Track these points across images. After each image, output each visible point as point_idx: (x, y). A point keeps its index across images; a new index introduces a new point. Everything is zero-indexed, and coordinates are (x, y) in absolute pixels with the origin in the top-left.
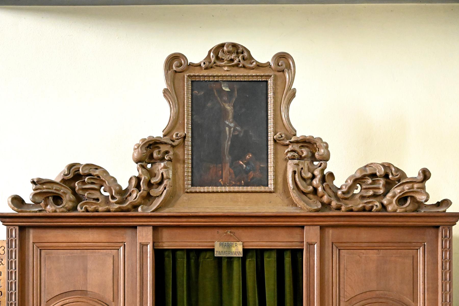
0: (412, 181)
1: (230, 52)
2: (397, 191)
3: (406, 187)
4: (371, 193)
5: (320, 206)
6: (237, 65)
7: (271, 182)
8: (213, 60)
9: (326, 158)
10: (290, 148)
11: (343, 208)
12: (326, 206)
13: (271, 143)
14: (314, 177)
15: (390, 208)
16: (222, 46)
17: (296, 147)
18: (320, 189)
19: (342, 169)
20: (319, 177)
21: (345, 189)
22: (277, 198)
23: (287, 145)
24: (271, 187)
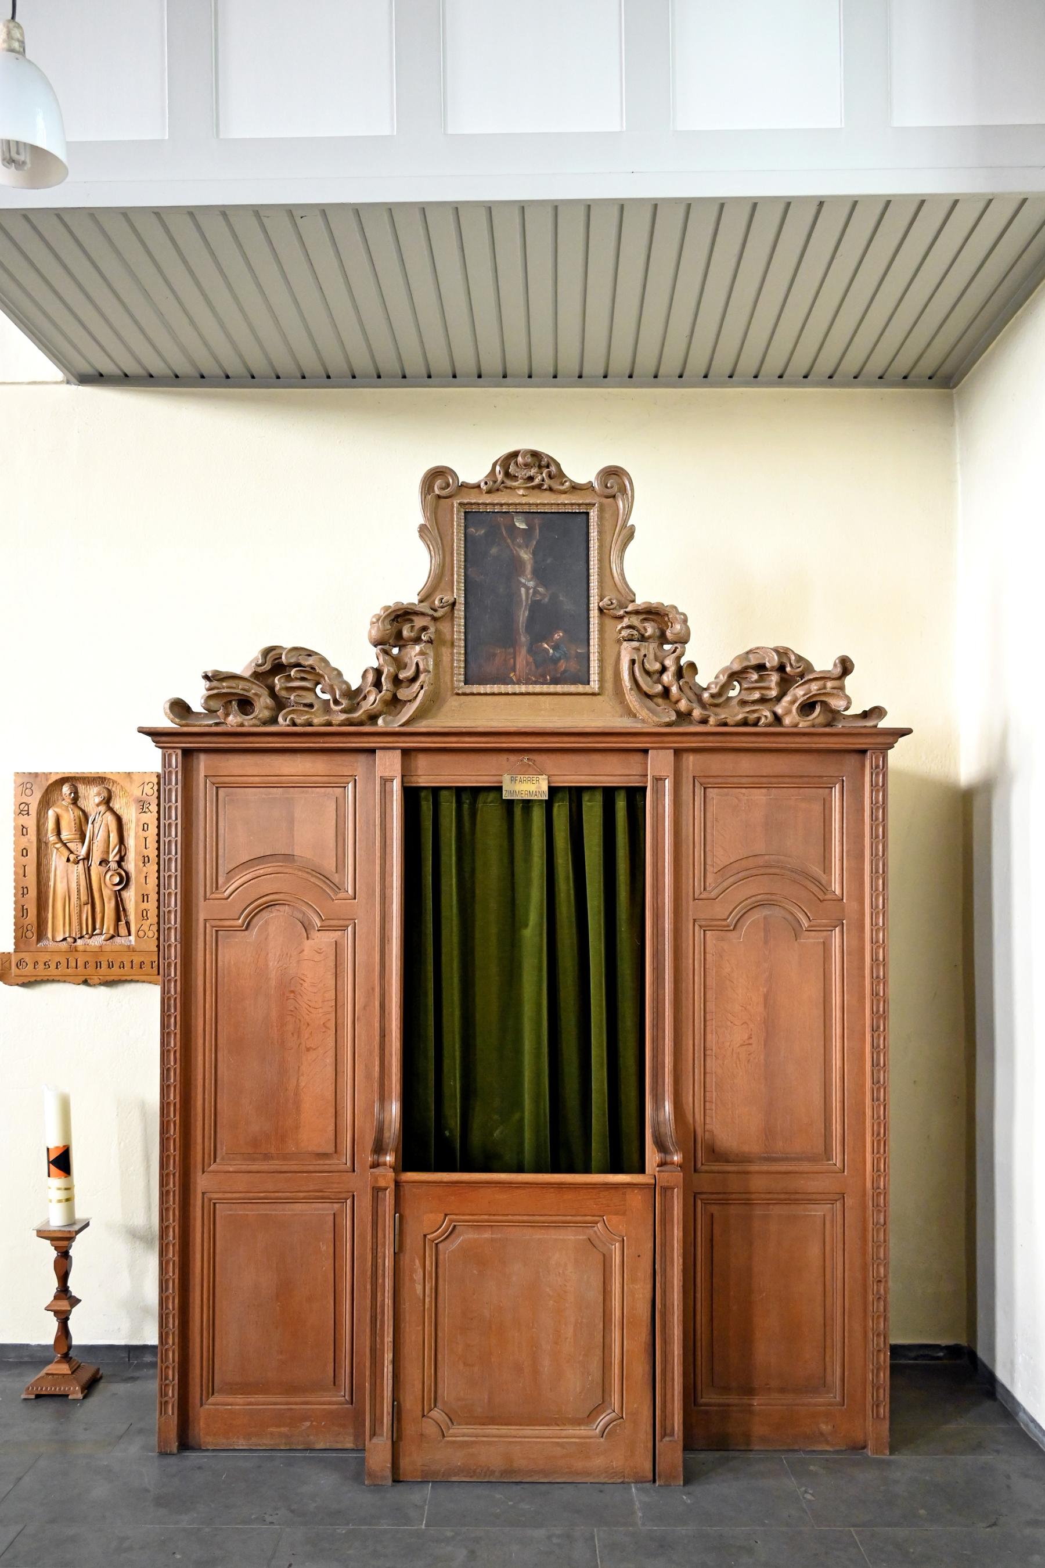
0: (823, 678)
2: (799, 693)
3: (814, 687)
4: (756, 695)
5: (674, 717)
6: (539, 487)
7: (594, 677)
9: (683, 640)
10: (626, 621)
11: (712, 720)
12: (684, 717)
13: (594, 614)
14: (664, 669)
15: (787, 721)
16: (515, 455)
17: (635, 621)
18: (674, 689)
19: (710, 657)
21: (714, 690)
23: (621, 618)
24: (594, 685)
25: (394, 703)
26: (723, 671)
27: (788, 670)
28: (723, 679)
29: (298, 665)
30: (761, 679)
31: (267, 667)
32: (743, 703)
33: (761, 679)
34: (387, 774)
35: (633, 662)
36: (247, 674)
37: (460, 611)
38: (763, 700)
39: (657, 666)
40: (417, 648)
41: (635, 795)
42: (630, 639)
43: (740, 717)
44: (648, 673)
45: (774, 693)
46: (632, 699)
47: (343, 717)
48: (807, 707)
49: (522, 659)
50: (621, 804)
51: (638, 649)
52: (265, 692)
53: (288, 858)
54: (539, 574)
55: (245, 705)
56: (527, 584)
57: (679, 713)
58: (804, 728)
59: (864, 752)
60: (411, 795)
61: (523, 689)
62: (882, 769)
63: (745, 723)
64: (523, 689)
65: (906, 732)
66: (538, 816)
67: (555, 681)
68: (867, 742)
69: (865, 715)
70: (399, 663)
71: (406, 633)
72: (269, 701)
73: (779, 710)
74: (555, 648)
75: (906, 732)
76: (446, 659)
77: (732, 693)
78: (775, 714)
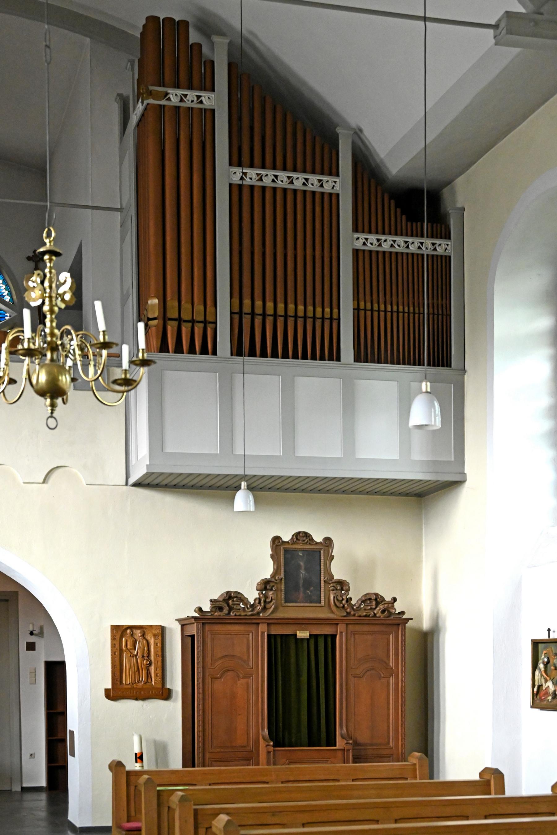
0: (388, 603)
1: (304, 537)
2: (381, 607)
3: (386, 606)
4: (369, 608)
5: (345, 614)
6: (306, 543)
7: (323, 602)
8: (295, 540)
9: (348, 590)
10: (332, 585)
11: (356, 615)
12: (348, 614)
13: (322, 582)
14: (343, 599)
15: (378, 615)
16: (299, 533)
17: (335, 585)
18: (346, 605)
19: (355, 595)
20: (345, 600)
21: (357, 606)
22: (326, 609)
23: (330, 584)
24: (323, 603)
25: (265, 609)
26: (359, 600)
27: (378, 599)
28: (359, 602)
29: (236, 597)
30: (370, 602)
31: (227, 598)
32: (365, 609)
33: (370, 602)
34: (264, 631)
35: (334, 597)
36: (221, 599)
37: (283, 581)
38: (371, 609)
39: (341, 599)
40: (272, 592)
41: (333, 637)
42: (333, 590)
43: (364, 614)
44: (338, 600)
45: (374, 607)
46: (334, 608)
47: (250, 613)
48: (383, 611)
49: (301, 595)
50: (329, 639)
51: (335, 593)
52: (226, 605)
53: (233, 656)
54: (306, 569)
55: (221, 609)
56: (303, 573)
57: (347, 612)
58: (382, 617)
59: (399, 625)
60: (269, 636)
61: (302, 605)
62: (404, 630)
63: (366, 616)
64: (302, 605)
65: (412, 619)
66: (305, 645)
67: (311, 602)
68: (398, 621)
69: (399, 613)
70: (266, 597)
71: (268, 587)
72: (228, 608)
73: (375, 612)
74: (311, 592)
75: (412, 619)
76: (279, 596)
77: (362, 606)
78: (374, 613)
